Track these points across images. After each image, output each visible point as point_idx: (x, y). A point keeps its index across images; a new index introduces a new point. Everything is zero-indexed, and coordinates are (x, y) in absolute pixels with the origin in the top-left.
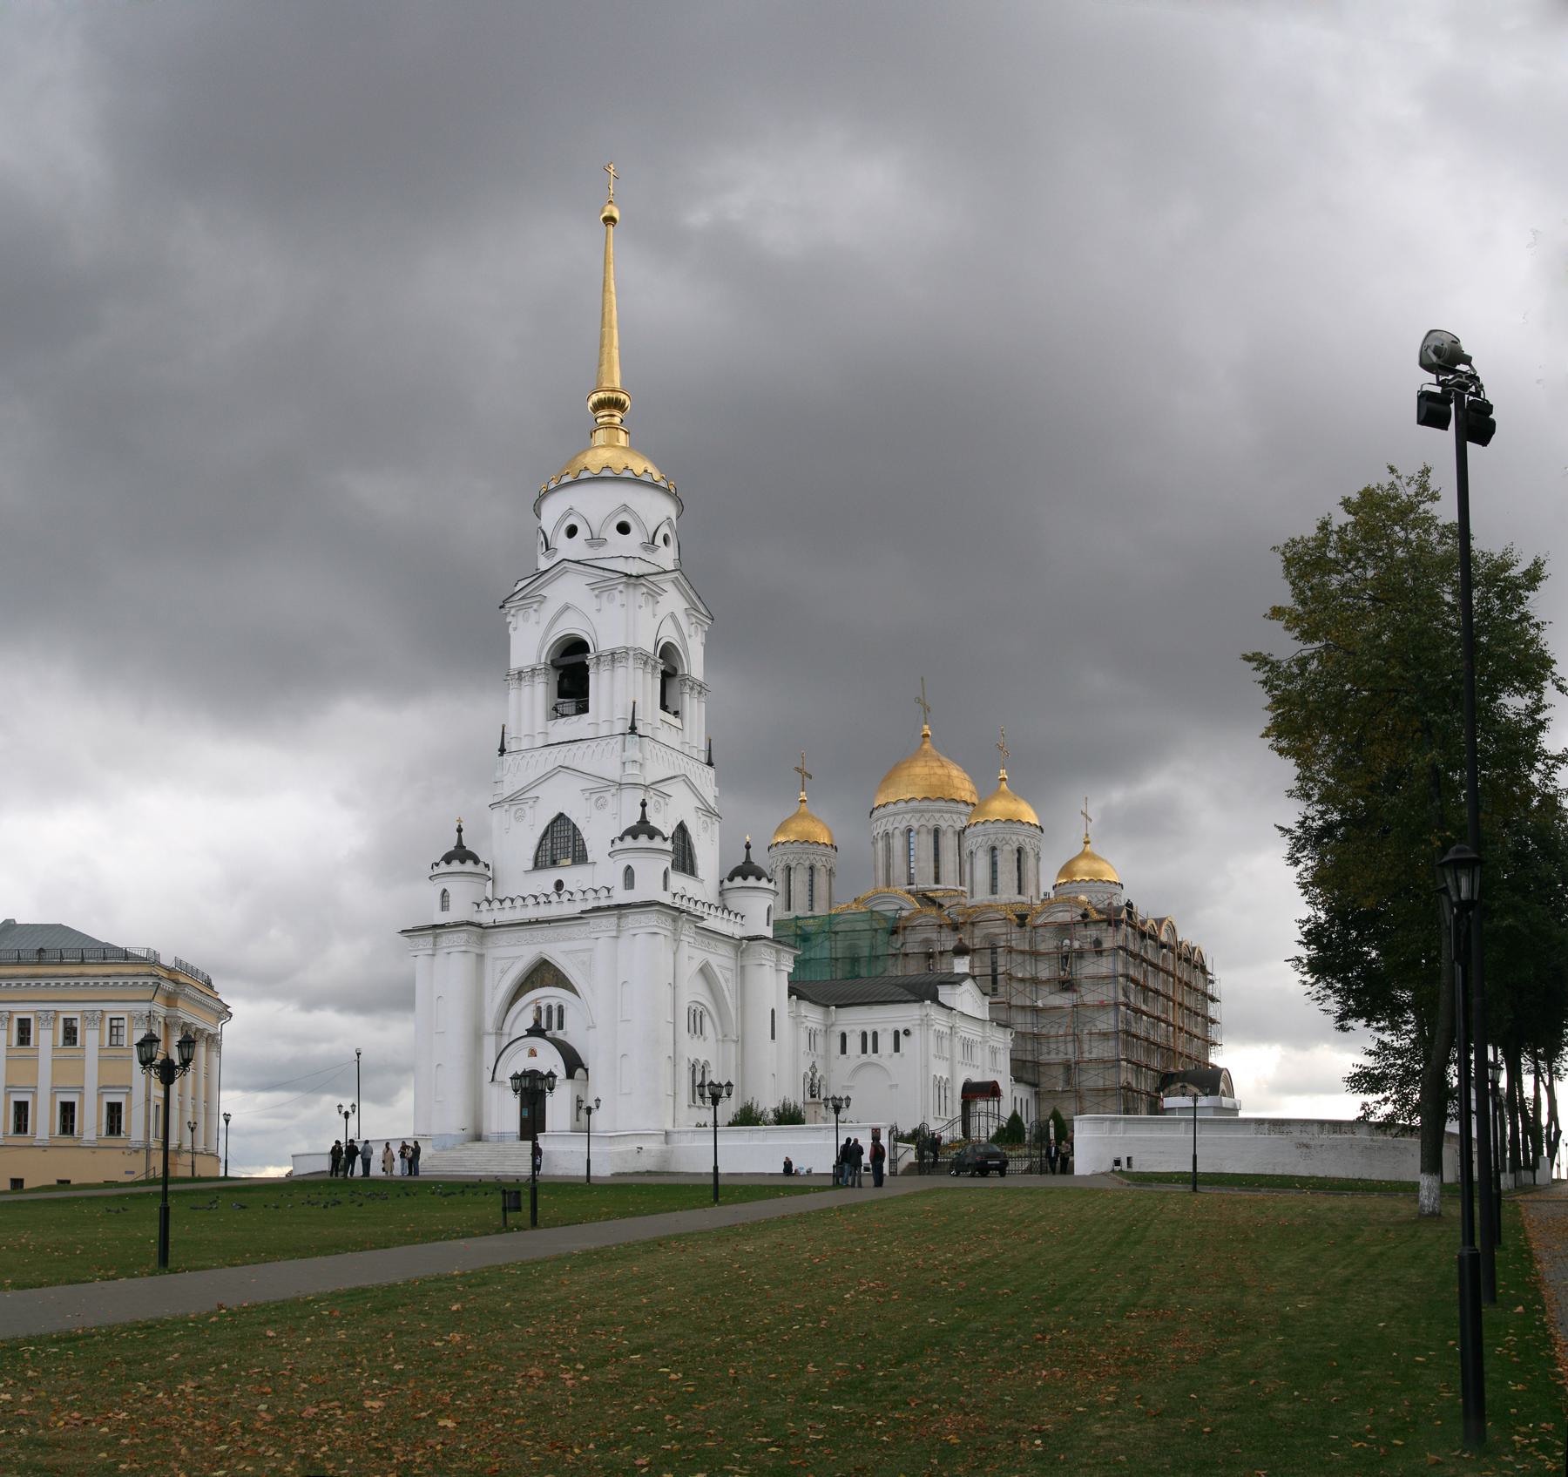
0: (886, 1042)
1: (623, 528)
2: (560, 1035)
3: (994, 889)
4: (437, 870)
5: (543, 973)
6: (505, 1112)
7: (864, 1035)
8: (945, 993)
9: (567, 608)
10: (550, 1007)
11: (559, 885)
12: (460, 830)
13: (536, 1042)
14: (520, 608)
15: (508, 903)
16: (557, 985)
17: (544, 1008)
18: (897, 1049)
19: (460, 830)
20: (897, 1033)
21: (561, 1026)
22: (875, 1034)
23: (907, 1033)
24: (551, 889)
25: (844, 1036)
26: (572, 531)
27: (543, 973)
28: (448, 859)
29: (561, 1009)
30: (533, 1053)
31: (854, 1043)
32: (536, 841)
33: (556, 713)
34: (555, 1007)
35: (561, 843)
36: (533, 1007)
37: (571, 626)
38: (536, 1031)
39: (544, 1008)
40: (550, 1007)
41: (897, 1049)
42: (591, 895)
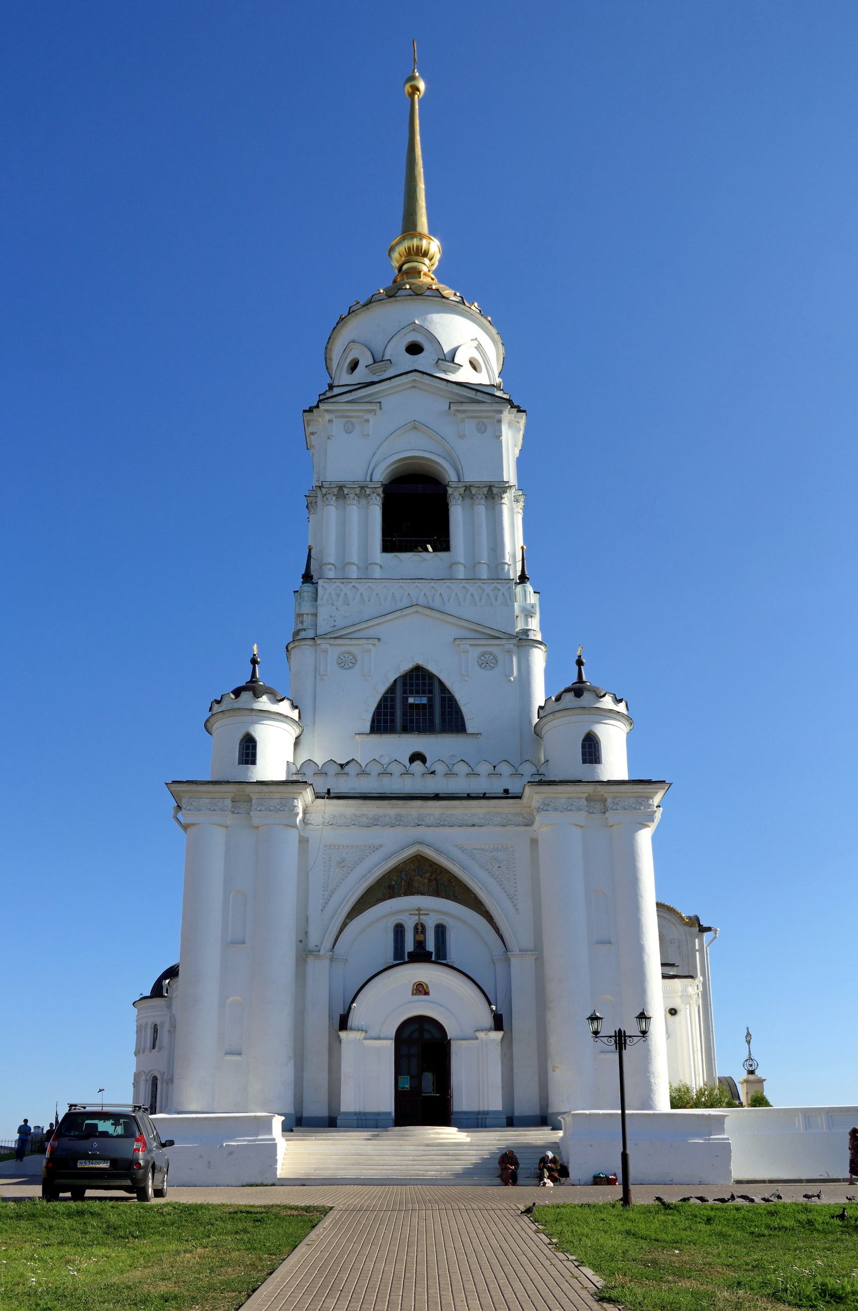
5: (418, 875)
10: (420, 929)
16: (437, 894)
29: (441, 930)
34: (430, 925)
36: (391, 923)
40: (420, 929)
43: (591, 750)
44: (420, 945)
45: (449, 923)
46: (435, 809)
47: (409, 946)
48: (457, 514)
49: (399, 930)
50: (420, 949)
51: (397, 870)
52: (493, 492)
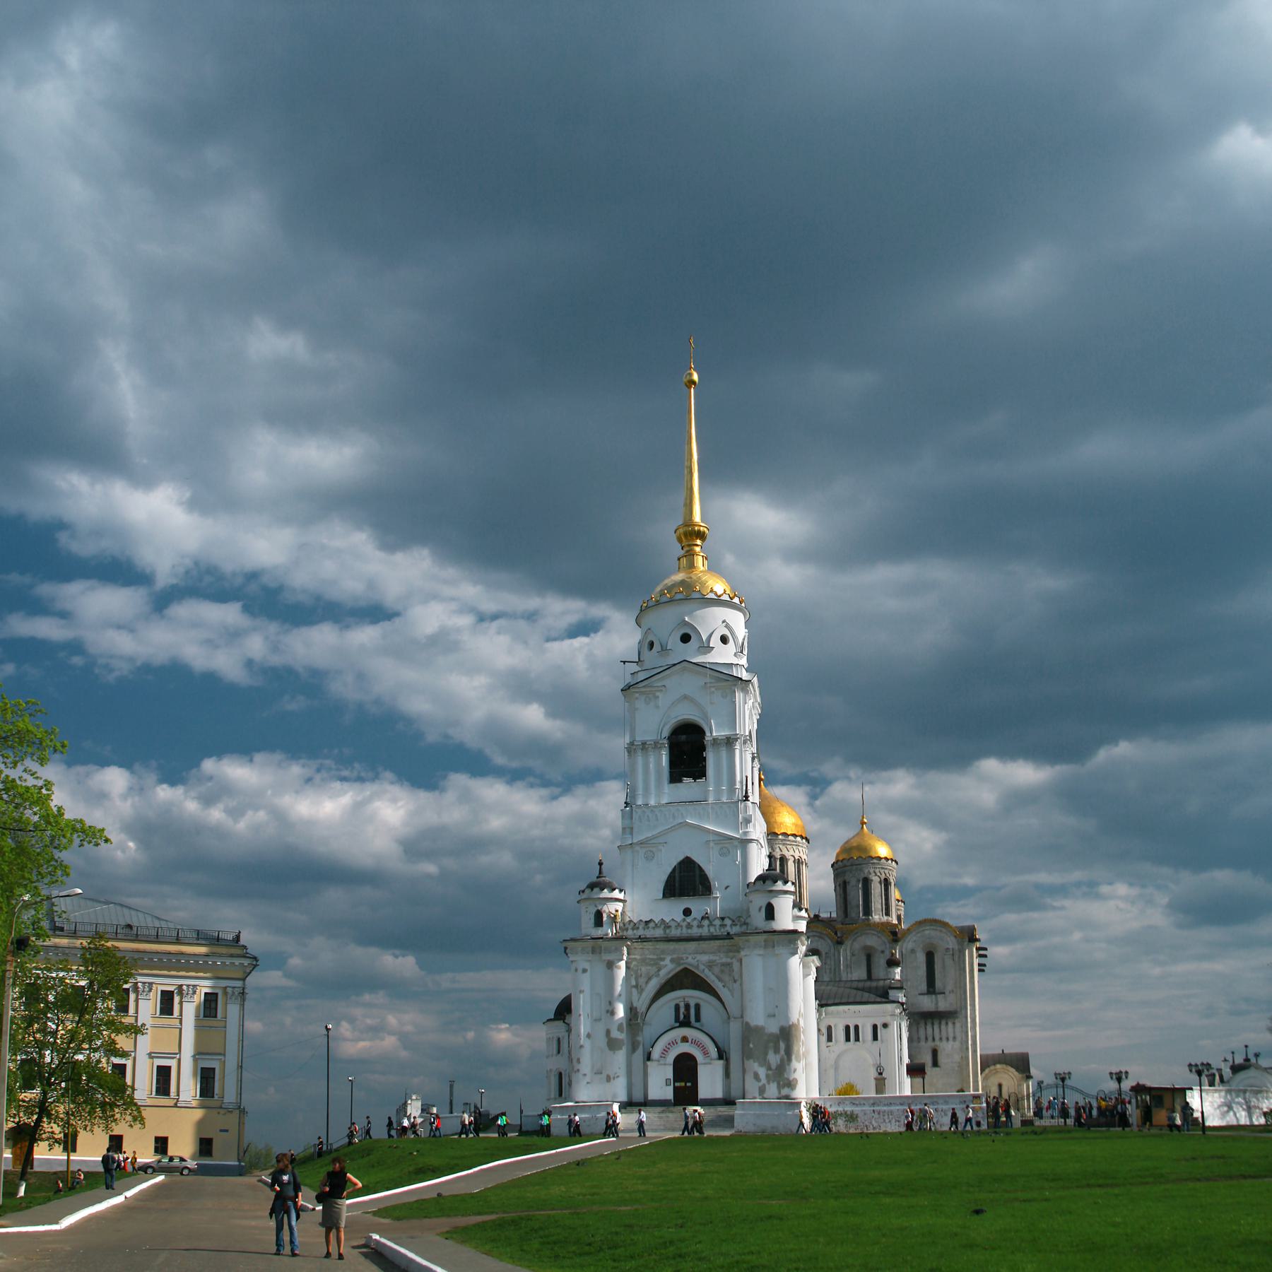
0: (866, 1033)
1: (724, 640)
2: (697, 1025)
3: (868, 911)
4: (584, 896)
5: (686, 979)
6: (660, 1084)
7: (847, 1028)
8: (892, 994)
9: (685, 697)
10: (687, 1007)
11: (687, 912)
12: (600, 864)
13: (685, 1031)
14: (642, 693)
15: (651, 925)
16: (695, 988)
17: (682, 1005)
18: (875, 1038)
19: (600, 864)
20: (875, 1027)
21: (698, 1019)
22: (857, 1027)
23: (885, 1026)
24: (679, 917)
25: (829, 1028)
26: (686, 638)
27: (686, 979)
28: (592, 886)
29: (698, 1007)
30: (685, 1039)
31: (839, 1034)
32: (665, 877)
33: (675, 778)
35: (687, 881)
36: (672, 1005)
37: (686, 713)
38: (685, 1023)
39: (682, 1005)
40: (687, 1007)
41: (875, 1038)
42: (728, 922)
43: (770, 912)
44: (687, 1016)
45: (702, 1004)
46: (692, 946)
47: (682, 1017)
48: (710, 756)
49: (677, 1007)
50: (685, 1019)
51: (676, 975)
52: (730, 742)
